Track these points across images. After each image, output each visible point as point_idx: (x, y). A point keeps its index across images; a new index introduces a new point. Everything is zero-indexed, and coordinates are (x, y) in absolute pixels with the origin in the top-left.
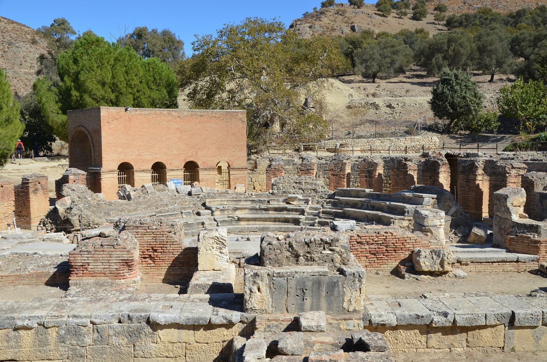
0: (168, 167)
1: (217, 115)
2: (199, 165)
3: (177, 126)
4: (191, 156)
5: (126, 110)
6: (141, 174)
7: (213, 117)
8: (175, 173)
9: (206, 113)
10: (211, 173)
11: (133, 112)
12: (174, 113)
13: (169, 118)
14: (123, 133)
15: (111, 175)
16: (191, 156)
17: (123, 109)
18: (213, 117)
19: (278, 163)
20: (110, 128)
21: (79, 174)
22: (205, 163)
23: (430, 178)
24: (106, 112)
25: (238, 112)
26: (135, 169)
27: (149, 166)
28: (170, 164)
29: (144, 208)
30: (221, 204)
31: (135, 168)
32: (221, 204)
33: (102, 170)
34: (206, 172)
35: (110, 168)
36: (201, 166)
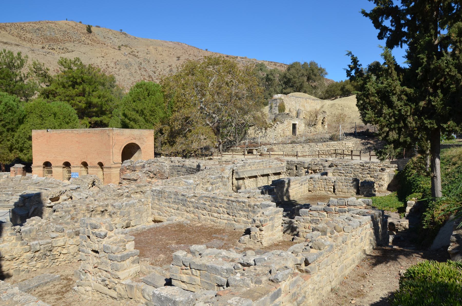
4: (84, 159)
5: (47, 131)
6: (56, 169)
8: (76, 169)
10: (95, 169)
12: (75, 132)
15: (39, 169)
16: (84, 159)
17: (46, 130)
22: (91, 163)
27: (61, 164)
31: (53, 165)
32: (34, 190)
34: (92, 169)
35: (38, 165)
36: (89, 165)
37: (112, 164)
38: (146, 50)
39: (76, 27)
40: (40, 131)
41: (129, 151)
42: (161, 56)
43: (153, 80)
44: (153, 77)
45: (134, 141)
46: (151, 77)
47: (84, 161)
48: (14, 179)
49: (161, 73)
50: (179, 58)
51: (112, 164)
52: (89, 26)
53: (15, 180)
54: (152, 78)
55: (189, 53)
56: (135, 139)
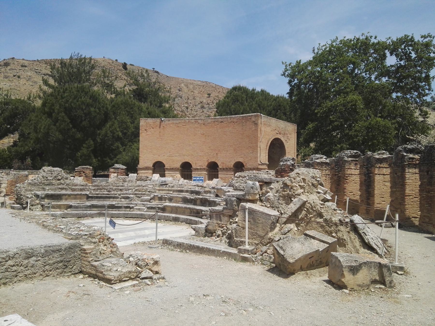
0: (194, 166)
1: (235, 120)
2: (219, 164)
3: (202, 132)
7: (230, 122)
9: (226, 120)
11: (167, 122)
13: (196, 125)
14: (157, 138)
18: (230, 122)
19: (285, 163)
20: (148, 135)
21: (118, 168)
22: (223, 163)
23: (428, 172)
24: (143, 122)
25: (252, 115)
26: (166, 167)
28: (196, 164)
29: (94, 190)
30: (168, 193)
32: (168, 193)
33: (139, 166)
35: (146, 165)
36: (220, 167)
37: (259, 165)
38: (179, 87)
39: (113, 64)
40: (150, 121)
41: (276, 148)
42: (192, 93)
43: (186, 115)
44: (186, 112)
45: (279, 136)
46: (184, 112)
47: (213, 160)
48: (127, 180)
49: (193, 109)
50: (209, 94)
51: (259, 165)
52: (125, 63)
53: (129, 181)
54: (185, 113)
55: (219, 91)
56: (280, 133)
